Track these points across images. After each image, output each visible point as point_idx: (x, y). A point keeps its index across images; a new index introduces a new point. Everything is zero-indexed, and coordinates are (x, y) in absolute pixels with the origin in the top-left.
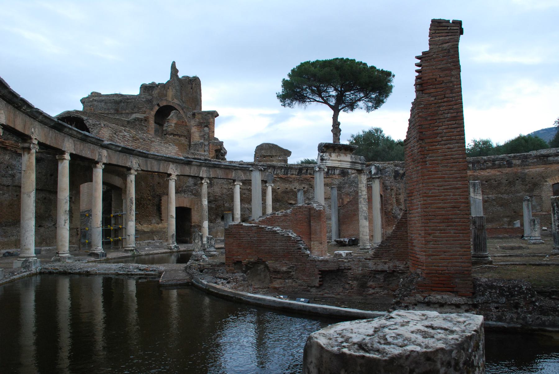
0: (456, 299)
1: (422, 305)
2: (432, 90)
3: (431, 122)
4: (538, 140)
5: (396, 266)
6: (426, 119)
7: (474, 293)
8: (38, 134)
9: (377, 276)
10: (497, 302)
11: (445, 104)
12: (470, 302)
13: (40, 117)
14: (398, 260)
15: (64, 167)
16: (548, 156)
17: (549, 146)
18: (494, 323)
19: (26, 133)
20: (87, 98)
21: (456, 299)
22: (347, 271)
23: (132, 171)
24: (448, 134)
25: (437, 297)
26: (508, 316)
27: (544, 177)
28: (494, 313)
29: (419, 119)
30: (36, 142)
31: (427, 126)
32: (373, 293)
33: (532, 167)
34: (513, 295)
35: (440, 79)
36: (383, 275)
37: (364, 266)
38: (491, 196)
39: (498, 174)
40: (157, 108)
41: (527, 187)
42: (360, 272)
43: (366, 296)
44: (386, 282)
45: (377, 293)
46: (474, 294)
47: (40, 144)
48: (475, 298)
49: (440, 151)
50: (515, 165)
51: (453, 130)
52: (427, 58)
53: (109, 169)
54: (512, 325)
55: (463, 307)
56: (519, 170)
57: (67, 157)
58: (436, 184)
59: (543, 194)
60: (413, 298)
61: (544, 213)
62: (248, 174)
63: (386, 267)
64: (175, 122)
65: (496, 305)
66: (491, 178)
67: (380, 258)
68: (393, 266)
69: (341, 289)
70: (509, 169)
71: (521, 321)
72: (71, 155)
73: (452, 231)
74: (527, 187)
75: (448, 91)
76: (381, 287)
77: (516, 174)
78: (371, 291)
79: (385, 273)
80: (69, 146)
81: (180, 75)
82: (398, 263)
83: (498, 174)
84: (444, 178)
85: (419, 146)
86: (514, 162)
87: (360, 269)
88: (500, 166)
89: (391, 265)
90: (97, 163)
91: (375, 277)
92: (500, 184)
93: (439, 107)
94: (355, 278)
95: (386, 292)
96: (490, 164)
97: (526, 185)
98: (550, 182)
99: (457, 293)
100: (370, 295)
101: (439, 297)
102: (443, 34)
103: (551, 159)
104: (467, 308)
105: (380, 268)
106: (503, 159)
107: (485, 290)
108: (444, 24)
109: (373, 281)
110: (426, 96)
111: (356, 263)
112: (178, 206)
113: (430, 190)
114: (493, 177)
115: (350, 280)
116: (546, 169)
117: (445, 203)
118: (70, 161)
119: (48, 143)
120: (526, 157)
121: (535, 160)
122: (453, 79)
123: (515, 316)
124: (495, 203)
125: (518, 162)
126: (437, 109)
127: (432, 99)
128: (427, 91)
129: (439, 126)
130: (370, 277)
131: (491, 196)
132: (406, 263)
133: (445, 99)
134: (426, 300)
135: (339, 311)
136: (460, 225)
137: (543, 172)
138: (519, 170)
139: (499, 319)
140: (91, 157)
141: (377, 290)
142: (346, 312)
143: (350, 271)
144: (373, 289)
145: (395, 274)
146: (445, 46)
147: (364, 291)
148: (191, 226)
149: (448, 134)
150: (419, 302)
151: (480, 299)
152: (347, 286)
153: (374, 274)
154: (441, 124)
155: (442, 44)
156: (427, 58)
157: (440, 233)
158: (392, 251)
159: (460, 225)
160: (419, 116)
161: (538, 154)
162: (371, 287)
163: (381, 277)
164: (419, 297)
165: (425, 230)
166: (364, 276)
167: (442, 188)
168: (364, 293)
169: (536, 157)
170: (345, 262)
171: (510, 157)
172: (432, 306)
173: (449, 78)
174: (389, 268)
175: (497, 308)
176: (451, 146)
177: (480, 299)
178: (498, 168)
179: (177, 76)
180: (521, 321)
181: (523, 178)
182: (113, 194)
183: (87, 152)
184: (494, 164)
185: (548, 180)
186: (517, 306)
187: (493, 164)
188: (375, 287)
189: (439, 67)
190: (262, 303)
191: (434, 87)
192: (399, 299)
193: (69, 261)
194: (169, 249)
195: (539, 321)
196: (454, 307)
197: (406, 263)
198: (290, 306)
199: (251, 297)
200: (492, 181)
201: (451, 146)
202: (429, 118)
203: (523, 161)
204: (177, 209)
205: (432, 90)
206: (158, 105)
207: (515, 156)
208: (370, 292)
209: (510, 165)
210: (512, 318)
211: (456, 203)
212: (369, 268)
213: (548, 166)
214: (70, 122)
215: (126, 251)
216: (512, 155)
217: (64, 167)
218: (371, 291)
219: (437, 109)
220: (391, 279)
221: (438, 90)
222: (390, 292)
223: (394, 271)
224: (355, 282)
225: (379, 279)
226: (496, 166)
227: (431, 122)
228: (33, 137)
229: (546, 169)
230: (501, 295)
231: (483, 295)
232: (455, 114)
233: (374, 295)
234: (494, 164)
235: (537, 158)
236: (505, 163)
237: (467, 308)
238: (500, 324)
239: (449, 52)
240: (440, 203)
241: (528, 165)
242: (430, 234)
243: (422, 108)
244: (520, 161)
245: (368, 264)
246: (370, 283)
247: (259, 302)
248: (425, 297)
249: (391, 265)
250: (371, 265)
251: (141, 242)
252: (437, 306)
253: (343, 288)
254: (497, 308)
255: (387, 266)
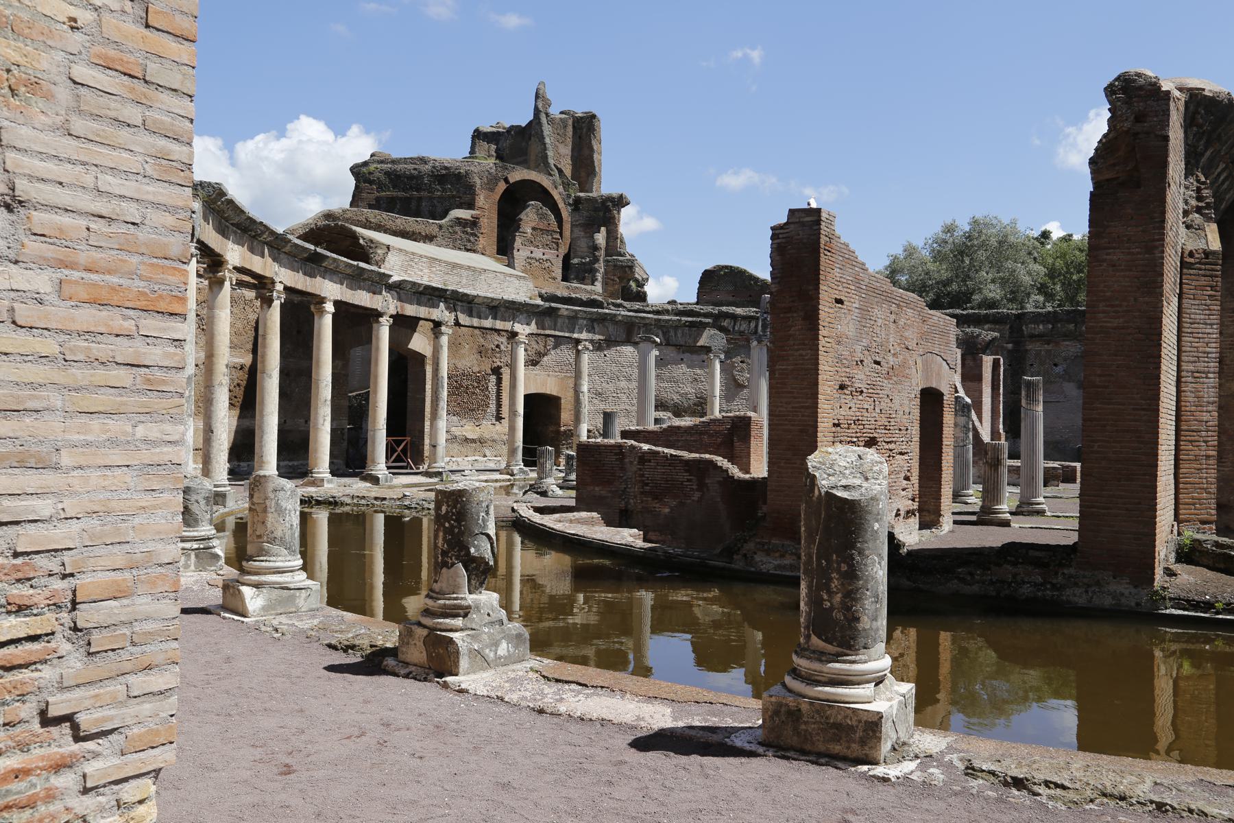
8: (285, 277)
13: (287, 249)
15: (326, 326)
19: (267, 275)
20: (365, 164)
23: (443, 328)
30: (279, 287)
40: (502, 186)
47: (286, 289)
53: (404, 325)
57: (330, 307)
62: (672, 333)
64: (533, 224)
72: (337, 303)
80: (331, 290)
81: (554, 111)
90: (380, 315)
112: (533, 390)
118: (334, 315)
119: (299, 287)
140: (369, 305)
148: (558, 432)
179: (547, 115)
182: (407, 369)
183: (362, 298)
193: (330, 486)
194: (508, 474)
204: (527, 397)
206: (506, 180)
214: (332, 241)
215: (427, 474)
217: (326, 326)
228: (277, 280)
251: (459, 459)
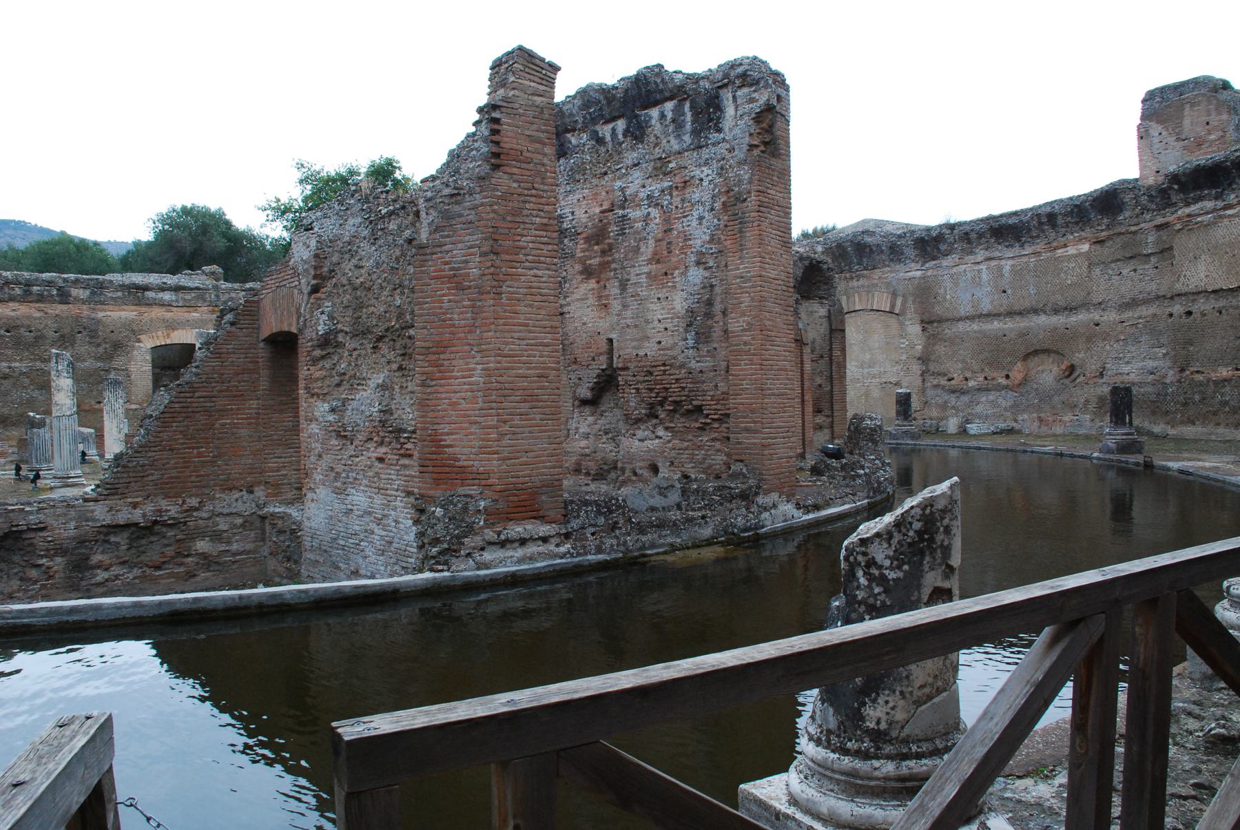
0: (544, 529)
1: (494, 548)
2: (515, 170)
3: (510, 225)
4: (101, 251)
5: (160, 511)
6: (504, 219)
7: (565, 516)
9: (113, 539)
10: (595, 525)
11: (533, 199)
12: (564, 531)
14: (167, 496)
16: (146, 288)
17: (119, 267)
18: (593, 557)
21: (544, 529)
22: (32, 535)
24: (535, 252)
25: (517, 530)
26: (609, 542)
27: (135, 331)
28: (591, 542)
29: (492, 215)
31: (507, 231)
32: (107, 580)
33: (111, 308)
34: (611, 512)
35: (528, 155)
36: (126, 535)
37: (84, 517)
38: (17, 364)
39: (38, 315)
41: (101, 350)
42: (72, 533)
43: (88, 590)
44: (133, 551)
45: (117, 577)
46: (566, 518)
48: (568, 522)
49: (523, 278)
50: (77, 299)
51: (542, 246)
52: (509, 111)
54: (614, 556)
55: (552, 540)
56: (85, 311)
58: (516, 335)
59: (133, 368)
60: (478, 538)
61: (134, 407)
63: (137, 516)
65: (593, 530)
66: (18, 322)
67: (124, 495)
68: (154, 511)
69: (15, 583)
70: (64, 307)
71: (622, 548)
73: (538, 417)
74: (101, 350)
75: (538, 179)
76: (124, 563)
77: (77, 318)
78: (101, 575)
79: (133, 529)
82: (164, 504)
83: (38, 315)
84: (527, 325)
85: (489, 264)
86: (75, 292)
87: (72, 525)
88: (41, 298)
89: (149, 508)
91: (108, 542)
92: (39, 338)
93: (525, 202)
94: (61, 551)
95: (136, 572)
96: (18, 291)
97: (99, 345)
98: (148, 343)
99: (542, 519)
100: (99, 584)
101: (520, 529)
102: (536, 79)
103: (150, 294)
104: (558, 540)
105: (122, 517)
106: (50, 283)
107: (580, 508)
108: (538, 62)
109: (102, 553)
110: (506, 176)
111: (59, 511)
113: (507, 344)
114: (27, 322)
115: (42, 557)
116: (141, 314)
117: (529, 369)
120: (101, 286)
121: (120, 294)
122: (545, 161)
123: (614, 542)
124: (27, 381)
125: (83, 294)
126: (521, 205)
127: (515, 185)
128: (507, 169)
129: (523, 236)
130: (97, 541)
131: (17, 364)
132: (184, 502)
133: (534, 192)
134: (503, 537)
135: (339, 589)
136: (548, 407)
137: (133, 321)
138: (85, 311)
139: (599, 550)
141: (116, 570)
142: (356, 587)
143: (41, 534)
144: (106, 570)
145: (157, 527)
146: (539, 100)
147: (82, 579)
149: (535, 252)
150: (490, 543)
151: (575, 524)
152: (33, 573)
153: (107, 534)
154: (525, 232)
155: (533, 94)
156: (509, 111)
157: (521, 420)
158: (151, 478)
159: (548, 407)
160: (494, 211)
161: (127, 282)
162: (99, 567)
163: (121, 539)
164: (490, 534)
165: (498, 415)
166: (81, 541)
167: (525, 342)
168: (84, 583)
169: (123, 287)
170: (31, 513)
171: (65, 280)
172: (508, 546)
173: (540, 157)
174: (144, 515)
175: (593, 534)
176: (540, 273)
177: (575, 524)
178: (37, 301)
180: (622, 548)
181: (92, 331)
184: (27, 293)
185: (142, 337)
186: (614, 526)
187: (25, 291)
188: (111, 565)
189: (527, 133)
190: (90, 617)
191: (519, 165)
192: (446, 546)
195: (639, 544)
196: (540, 543)
197: (184, 502)
198: (195, 606)
199: (22, 611)
200: (22, 330)
201: (540, 273)
202: (509, 218)
203: (93, 293)
205: (515, 170)
207: (77, 281)
208: (99, 579)
209: (64, 297)
210: (612, 546)
211: (544, 368)
212: (94, 520)
213: (143, 309)
216: (72, 276)
218: (101, 575)
219: (521, 205)
220: (143, 542)
221: (525, 172)
222: (148, 571)
223: (155, 522)
224: (59, 560)
225: (117, 544)
226: (35, 298)
227: (510, 225)
229: (141, 314)
230: (599, 513)
231: (578, 516)
232: (545, 221)
233: (110, 584)
234: (27, 293)
235: (123, 291)
236: (55, 292)
237: (558, 540)
238: (601, 557)
239: (542, 112)
240: (520, 368)
241: (102, 303)
242: (505, 422)
243: (499, 198)
244: (88, 292)
245: (93, 511)
246: (97, 558)
247: (75, 618)
248: (499, 534)
249: (149, 508)
250: (101, 513)
252: (517, 544)
253: (21, 579)
254: (593, 534)
255: (138, 512)
